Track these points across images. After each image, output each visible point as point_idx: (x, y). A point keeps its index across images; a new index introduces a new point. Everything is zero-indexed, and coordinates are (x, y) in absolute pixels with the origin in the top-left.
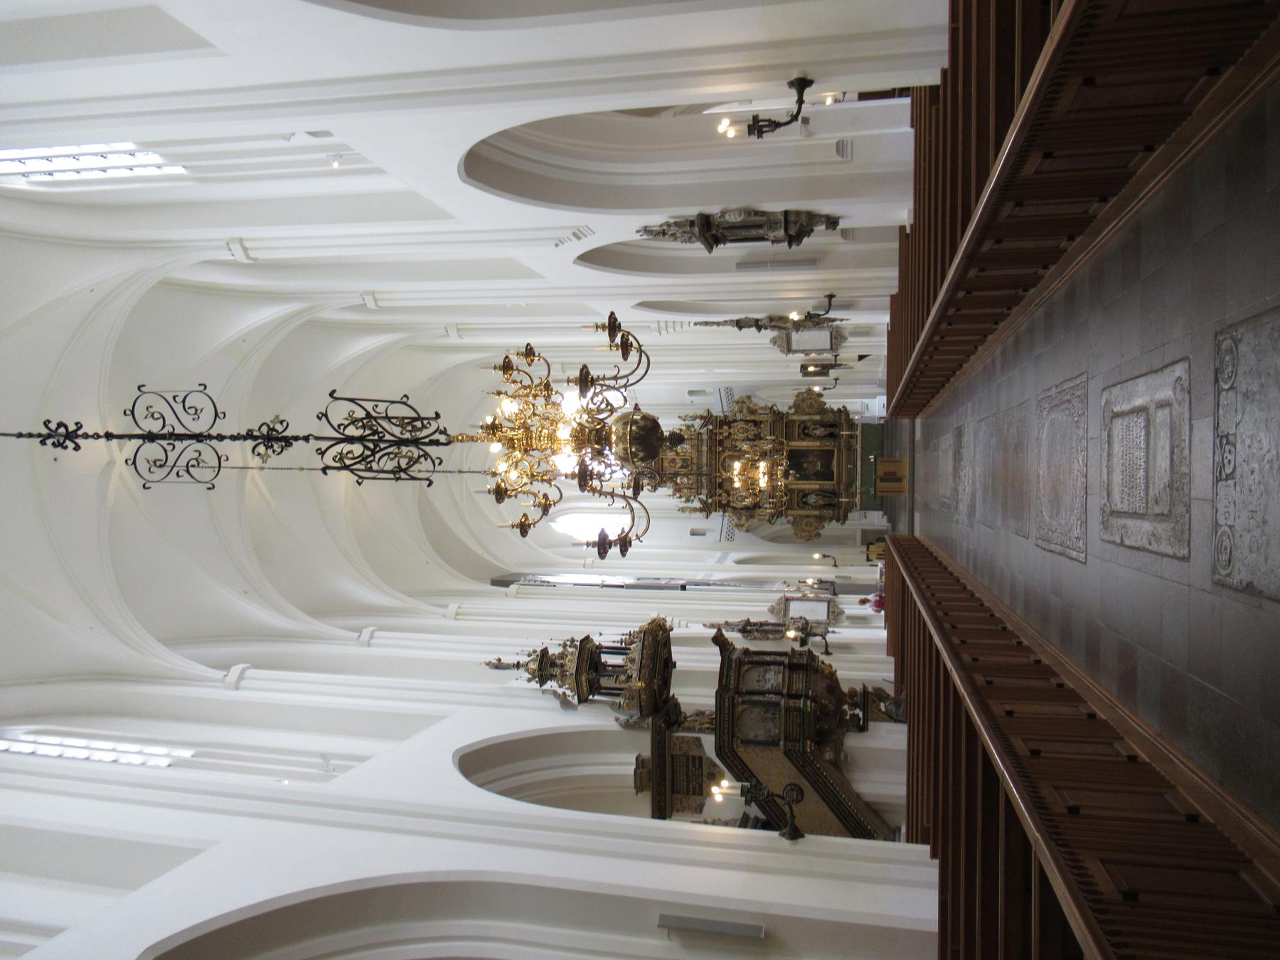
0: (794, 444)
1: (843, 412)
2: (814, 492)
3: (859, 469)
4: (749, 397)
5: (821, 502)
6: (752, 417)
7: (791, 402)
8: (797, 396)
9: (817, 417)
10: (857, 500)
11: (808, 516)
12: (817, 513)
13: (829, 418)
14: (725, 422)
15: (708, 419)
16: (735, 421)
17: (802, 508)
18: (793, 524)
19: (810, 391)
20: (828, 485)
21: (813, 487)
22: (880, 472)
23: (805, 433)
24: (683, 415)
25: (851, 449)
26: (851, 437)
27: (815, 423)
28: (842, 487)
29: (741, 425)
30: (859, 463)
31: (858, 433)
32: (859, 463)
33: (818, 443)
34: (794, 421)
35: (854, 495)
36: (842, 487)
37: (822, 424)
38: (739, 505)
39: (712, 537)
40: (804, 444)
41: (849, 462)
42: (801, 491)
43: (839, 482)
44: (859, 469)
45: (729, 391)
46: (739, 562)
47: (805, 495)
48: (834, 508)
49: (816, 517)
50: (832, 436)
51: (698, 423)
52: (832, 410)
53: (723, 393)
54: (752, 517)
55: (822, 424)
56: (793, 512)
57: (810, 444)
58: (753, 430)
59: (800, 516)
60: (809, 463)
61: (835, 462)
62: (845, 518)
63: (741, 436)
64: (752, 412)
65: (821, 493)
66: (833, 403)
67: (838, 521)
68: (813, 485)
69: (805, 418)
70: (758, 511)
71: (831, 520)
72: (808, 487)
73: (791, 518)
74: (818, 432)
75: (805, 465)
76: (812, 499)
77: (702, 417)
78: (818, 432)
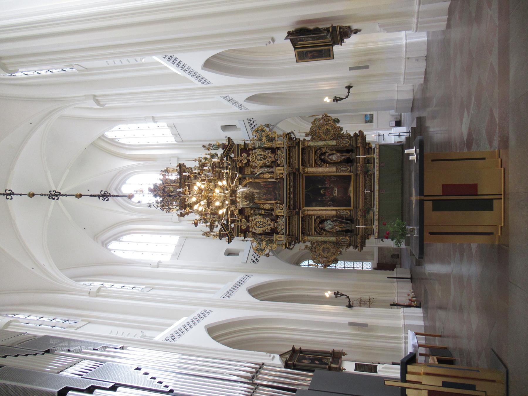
0: (310, 170)
1: (360, 136)
2: (330, 218)
3: (376, 194)
4: (268, 126)
5: (338, 228)
6: (269, 145)
7: (307, 127)
8: (314, 123)
9: (334, 143)
10: (375, 227)
11: (325, 242)
12: (333, 239)
13: (345, 143)
14: (245, 150)
15: (229, 147)
16: (254, 148)
17: (319, 234)
18: (311, 249)
19: (326, 117)
20: (344, 211)
21: (329, 213)
22: (434, 188)
23: (322, 161)
24: (206, 143)
25: (367, 173)
26: (368, 161)
27: (332, 148)
28: (359, 213)
29: (259, 152)
30: (376, 188)
31: (375, 156)
32: (376, 188)
33: (334, 169)
34: (310, 147)
35: (372, 222)
36: (359, 213)
37: (338, 150)
38: (259, 230)
39: (243, 256)
40: (320, 169)
41: (366, 187)
42: (319, 217)
43: (356, 208)
44: (376, 194)
45: (252, 122)
46: (254, 292)
47: (322, 221)
48: (349, 236)
49: (333, 243)
50: (349, 161)
51: (220, 152)
52: (349, 136)
53: (248, 125)
54: (271, 241)
55: (338, 150)
56: (309, 238)
57: (326, 169)
58: (270, 157)
59: (317, 242)
60: (326, 189)
61: (352, 188)
62: (363, 244)
63: (259, 163)
64: (271, 140)
65: (338, 219)
66: (350, 128)
67: (355, 247)
68: (330, 211)
69: (321, 143)
70: (276, 237)
71: (348, 246)
72: (324, 212)
73: (309, 244)
74: (334, 158)
75: (322, 191)
76: (328, 225)
77: (224, 146)
78: (334, 158)
